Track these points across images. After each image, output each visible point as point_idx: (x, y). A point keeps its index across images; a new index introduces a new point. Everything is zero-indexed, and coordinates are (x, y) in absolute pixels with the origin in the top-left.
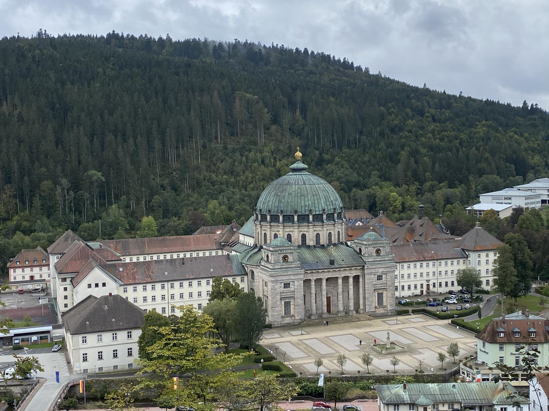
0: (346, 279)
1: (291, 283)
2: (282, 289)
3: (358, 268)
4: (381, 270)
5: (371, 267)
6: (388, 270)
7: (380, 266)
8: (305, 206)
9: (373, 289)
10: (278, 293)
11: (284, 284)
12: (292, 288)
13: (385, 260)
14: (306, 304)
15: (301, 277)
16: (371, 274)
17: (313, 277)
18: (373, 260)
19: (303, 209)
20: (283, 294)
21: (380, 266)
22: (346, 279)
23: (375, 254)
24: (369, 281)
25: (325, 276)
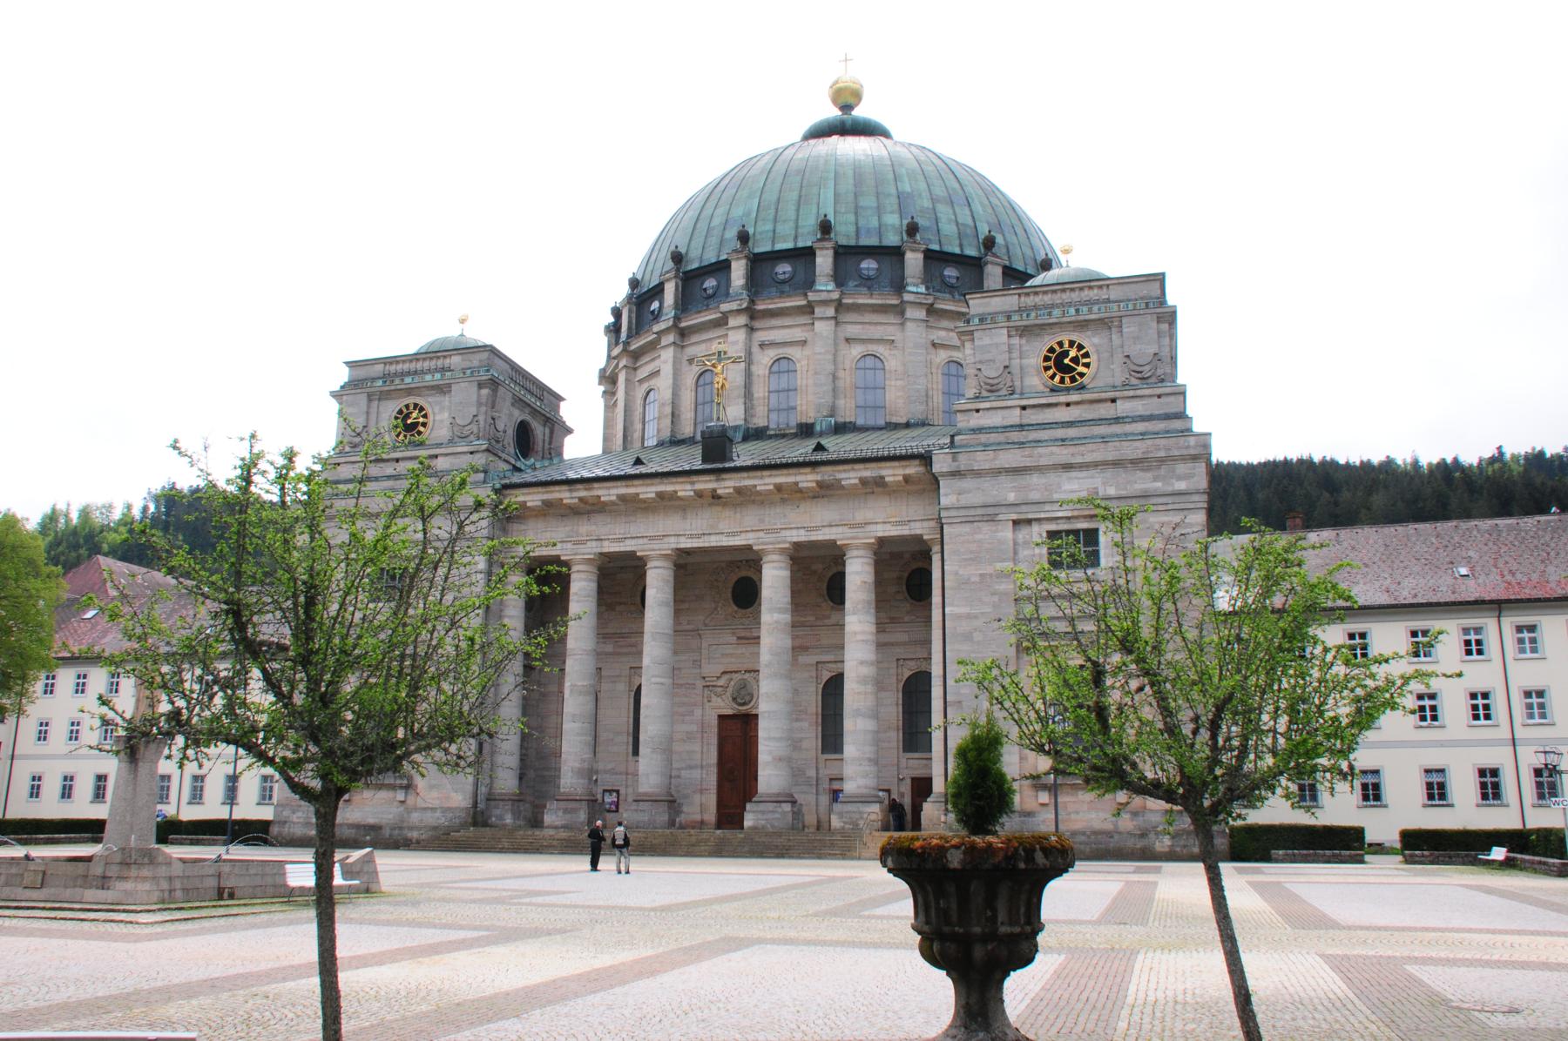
0: (819, 574)
3: (893, 473)
4: (1074, 486)
5: (982, 460)
6: (1143, 482)
7: (1063, 454)
13: (1117, 420)
16: (989, 514)
17: (579, 545)
18: (1014, 417)
19: (714, 241)
21: (1063, 454)
22: (819, 574)
24: (972, 572)
25: (657, 539)
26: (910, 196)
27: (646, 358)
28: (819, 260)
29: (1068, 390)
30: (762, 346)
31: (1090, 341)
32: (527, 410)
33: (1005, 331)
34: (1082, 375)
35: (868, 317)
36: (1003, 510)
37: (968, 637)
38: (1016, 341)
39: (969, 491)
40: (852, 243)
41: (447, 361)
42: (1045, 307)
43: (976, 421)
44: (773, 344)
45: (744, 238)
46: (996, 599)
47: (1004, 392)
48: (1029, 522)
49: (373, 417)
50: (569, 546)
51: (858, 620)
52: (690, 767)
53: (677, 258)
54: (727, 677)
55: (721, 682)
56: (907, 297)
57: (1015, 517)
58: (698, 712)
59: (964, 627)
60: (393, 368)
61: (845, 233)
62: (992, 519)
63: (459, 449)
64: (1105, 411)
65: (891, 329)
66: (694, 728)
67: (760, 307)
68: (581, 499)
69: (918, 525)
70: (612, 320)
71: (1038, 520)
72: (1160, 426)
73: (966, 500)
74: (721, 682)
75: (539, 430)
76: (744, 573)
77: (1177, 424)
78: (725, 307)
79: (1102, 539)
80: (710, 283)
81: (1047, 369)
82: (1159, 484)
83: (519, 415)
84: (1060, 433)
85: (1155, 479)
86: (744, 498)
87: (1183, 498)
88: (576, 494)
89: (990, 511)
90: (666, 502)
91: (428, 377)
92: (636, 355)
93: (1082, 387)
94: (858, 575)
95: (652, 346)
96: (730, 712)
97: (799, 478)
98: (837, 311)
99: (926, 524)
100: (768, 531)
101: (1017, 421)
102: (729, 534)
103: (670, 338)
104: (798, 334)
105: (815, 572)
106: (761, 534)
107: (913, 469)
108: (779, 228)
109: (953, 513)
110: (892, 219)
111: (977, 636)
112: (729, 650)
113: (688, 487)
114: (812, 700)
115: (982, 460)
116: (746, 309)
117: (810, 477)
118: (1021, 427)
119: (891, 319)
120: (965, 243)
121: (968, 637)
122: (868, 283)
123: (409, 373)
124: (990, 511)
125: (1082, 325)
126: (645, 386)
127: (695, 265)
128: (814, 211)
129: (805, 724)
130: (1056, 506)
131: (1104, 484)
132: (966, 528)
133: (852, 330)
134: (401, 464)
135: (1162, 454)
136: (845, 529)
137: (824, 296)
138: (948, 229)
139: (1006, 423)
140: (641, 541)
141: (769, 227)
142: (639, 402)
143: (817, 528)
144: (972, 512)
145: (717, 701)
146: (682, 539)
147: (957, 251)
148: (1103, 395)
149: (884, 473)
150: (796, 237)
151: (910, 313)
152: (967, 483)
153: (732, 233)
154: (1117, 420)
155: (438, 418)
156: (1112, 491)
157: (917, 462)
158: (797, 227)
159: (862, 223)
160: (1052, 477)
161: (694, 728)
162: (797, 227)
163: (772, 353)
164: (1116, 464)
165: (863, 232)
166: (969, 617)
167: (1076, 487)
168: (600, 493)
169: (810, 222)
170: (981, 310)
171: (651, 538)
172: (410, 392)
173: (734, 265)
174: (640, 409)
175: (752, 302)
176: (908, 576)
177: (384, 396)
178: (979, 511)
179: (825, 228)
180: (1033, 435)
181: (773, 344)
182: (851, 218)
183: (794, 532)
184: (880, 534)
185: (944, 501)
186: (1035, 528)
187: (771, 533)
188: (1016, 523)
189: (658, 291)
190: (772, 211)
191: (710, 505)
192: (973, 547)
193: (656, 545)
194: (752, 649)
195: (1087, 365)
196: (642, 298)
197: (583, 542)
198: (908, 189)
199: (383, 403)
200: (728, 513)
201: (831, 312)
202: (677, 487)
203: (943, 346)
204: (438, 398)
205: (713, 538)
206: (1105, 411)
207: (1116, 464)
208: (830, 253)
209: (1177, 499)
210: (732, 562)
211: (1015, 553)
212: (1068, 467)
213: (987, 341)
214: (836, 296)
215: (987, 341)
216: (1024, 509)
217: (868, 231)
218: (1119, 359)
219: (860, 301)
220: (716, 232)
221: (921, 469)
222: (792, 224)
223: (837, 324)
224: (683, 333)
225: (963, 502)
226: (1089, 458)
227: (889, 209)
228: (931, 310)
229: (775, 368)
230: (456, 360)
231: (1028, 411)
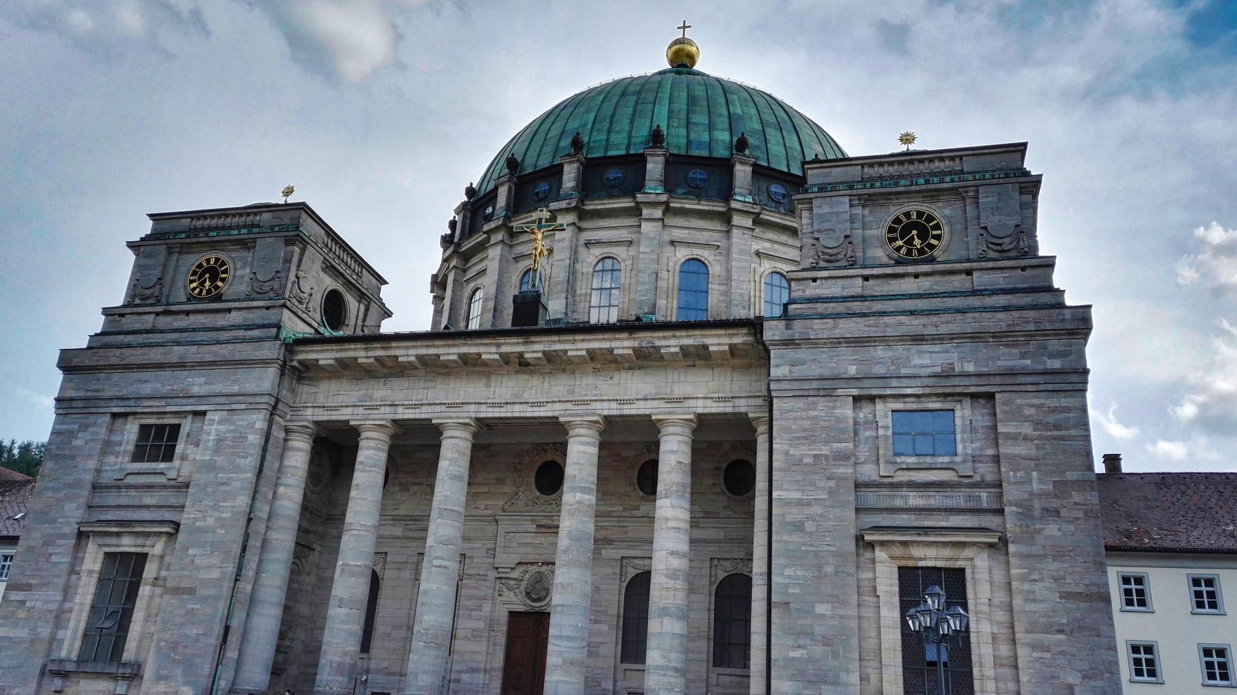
1: (184, 430)
2: (120, 463)
3: (717, 342)
4: (927, 360)
6: (1007, 358)
7: (913, 325)
8: (561, 136)
9: (849, 522)
10: (76, 485)
11: (145, 429)
12: (190, 456)
14: (376, 643)
15: (250, 387)
16: (827, 387)
17: (372, 409)
18: (856, 287)
19: (548, 149)
20: (112, 498)
21: (913, 325)
22: (630, 454)
23: (879, 253)
24: (805, 452)
25: (458, 405)
26: (741, 118)
27: (475, 260)
28: (649, 166)
29: (916, 262)
30: (588, 244)
31: (941, 212)
32: (341, 280)
33: (847, 199)
34: (932, 247)
35: (695, 222)
36: (843, 384)
37: (798, 527)
38: (858, 210)
39: (803, 363)
40: (683, 152)
41: (258, 218)
42: (891, 177)
43: (812, 290)
44: (599, 243)
45: (577, 144)
46: (832, 483)
47: (844, 263)
48: (872, 399)
49: (171, 270)
50: (361, 410)
51: (671, 509)
52: (473, 670)
53: (512, 164)
54: (521, 568)
55: (515, 575)
56: (734, 205)
57: (855, 392)
58: (487, 607)
59: (794, 514)
60: (200, 223)
61: (676, 139)
62: (829, 394)
63: (255, 304)
64: (958, 282)
65: (716, 236)
66: (481, 625)
67: (590, 206)
68: (377, 358)
69: (743, 402)
70: (449, 232)
71: (883, 397)
72: (1026, 299)
73: (798, 372)
74: (515, 575)
75: (353, 305)
76: (550, 457)
77: (1046, 298)
78: (554, 206)
79: (958, 422)
80: (543, 187)
81: (892, 240)
82: (1028, 362)
83: (330, 283)
84: (908, 304)
85: (1023, 356)
86: (555, 363)
87: (1058, 378)
88: (371, 354)
89: (828, 384)
90: (471, 366)
91: (233, 232)
92: (466, 257)
93: (932, 260)
94: (674, 454)
95: (482, 247)
96: (522, 608)
97: (614, 344)
98: (664, 213)
99: (752, 401)
100: (576, 403)
101: (858, 291)
102: (533, 404)
103: (499, 236)
104: (624, 235)
105: (625, 459)
106: (569, 406)
107: (740, 338)
108: (613, 137)
109: (785, 385)
110: (723, 136)
111: (810, 526)
112: (527, 539)
113: (494, 349)
114: (614, 600)
115: (820, 329)
116: (575, 209)
117: (627, 343)
118: (862, 298)
119: (717, 225)
120: (791, 163)
121: (798, 527)
122: (697, 192)
123: (217, 228)
124: (828, 384)
125: (933, 195)
126: (472, 285)
127: (530, 170)
128: (648, 123)
129: (604, 627)
130: (905, 382)
131: (961, 359)
132: (799, 403)
133: (678, 234)
134: (192, 317)
135: (1032, 327)
136: (662, 404)
137: (652, 198)
138: (776, 149)
139: (845, 293)
140: (438, 408)
141: (603, 136)
142: (465, 300)
143: (629, 402)
144: (807, 385)
145: (509, 596)
146: (483, 408)
147: (785, 169)
148: (958, 266)
149: (708, 341)
150: (628, 146)
151: (737, 220)
152: (802, 354)
153: (566, 142)
154: (974, 293)
155: (239, 273)
156: (970, 368)
157: (745, 331)
158: (630, 137)
159: (693, 136)
160: (900, 350)
161: (481, 625)
162: (630, 137)
163: (597, 252)
164: (975, 337)
165: (694, 145)
166: (800, 503)
167: (927, 362)
168: (397, 352)
169: (642, 132)
170: (820, 180)
171: (449, 405)
172: (213, 245)
173: (566, 168)
174: (465, 308)
175: (582, 201)
176: (730, 462)
177: (186, 249)
178: (815, 385)
179: (656, 138)
180: (878, 306)
181: (599, 243)
182: (683, 131)
183: (605, 405)
184: (700, 411)
185: (774, 372)
186: (880, 406)
187: (580, 401)
188: (856, 399)
189: (492, 196)
190: (607, 124)
191: (516, 372)
192: (807, 424)
193: (453, 412)
194: (551, 539)
195: (938, 237)
196: (476, 205)
197: (376, 407)
198: (739, 111)
199: (185, 257)
200: (536, 381)
201: (658, 213)
202: (482, 349)
203: (768, 256)
204: (243, 254)
205: (517, 408)
206: (958, 282)
207: (975, 337)
208: (662, 159)
209: (1049, 378)
210: (538, 445)
211: (856, 433)
212: (918, 339)
213: (826, 209)
214: (664, 198)
215: (826, 209)
216: (866, 383)
217: (700, 144)
218: (973, 231)
219: (688, 206)
220: (552, 142)
221: (750, 339)
222: (625, 134)
223: (664, 226)
224: (512, 234)
225: (796, 375)
226: (943, 330)
227: (720, 126)
228: (758, 221)
229: (599, 267)
230: (267, 216)
231: (871, 282)
